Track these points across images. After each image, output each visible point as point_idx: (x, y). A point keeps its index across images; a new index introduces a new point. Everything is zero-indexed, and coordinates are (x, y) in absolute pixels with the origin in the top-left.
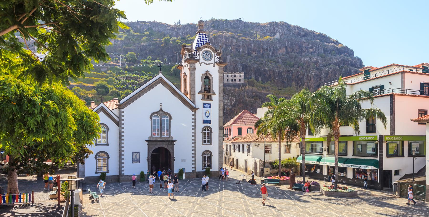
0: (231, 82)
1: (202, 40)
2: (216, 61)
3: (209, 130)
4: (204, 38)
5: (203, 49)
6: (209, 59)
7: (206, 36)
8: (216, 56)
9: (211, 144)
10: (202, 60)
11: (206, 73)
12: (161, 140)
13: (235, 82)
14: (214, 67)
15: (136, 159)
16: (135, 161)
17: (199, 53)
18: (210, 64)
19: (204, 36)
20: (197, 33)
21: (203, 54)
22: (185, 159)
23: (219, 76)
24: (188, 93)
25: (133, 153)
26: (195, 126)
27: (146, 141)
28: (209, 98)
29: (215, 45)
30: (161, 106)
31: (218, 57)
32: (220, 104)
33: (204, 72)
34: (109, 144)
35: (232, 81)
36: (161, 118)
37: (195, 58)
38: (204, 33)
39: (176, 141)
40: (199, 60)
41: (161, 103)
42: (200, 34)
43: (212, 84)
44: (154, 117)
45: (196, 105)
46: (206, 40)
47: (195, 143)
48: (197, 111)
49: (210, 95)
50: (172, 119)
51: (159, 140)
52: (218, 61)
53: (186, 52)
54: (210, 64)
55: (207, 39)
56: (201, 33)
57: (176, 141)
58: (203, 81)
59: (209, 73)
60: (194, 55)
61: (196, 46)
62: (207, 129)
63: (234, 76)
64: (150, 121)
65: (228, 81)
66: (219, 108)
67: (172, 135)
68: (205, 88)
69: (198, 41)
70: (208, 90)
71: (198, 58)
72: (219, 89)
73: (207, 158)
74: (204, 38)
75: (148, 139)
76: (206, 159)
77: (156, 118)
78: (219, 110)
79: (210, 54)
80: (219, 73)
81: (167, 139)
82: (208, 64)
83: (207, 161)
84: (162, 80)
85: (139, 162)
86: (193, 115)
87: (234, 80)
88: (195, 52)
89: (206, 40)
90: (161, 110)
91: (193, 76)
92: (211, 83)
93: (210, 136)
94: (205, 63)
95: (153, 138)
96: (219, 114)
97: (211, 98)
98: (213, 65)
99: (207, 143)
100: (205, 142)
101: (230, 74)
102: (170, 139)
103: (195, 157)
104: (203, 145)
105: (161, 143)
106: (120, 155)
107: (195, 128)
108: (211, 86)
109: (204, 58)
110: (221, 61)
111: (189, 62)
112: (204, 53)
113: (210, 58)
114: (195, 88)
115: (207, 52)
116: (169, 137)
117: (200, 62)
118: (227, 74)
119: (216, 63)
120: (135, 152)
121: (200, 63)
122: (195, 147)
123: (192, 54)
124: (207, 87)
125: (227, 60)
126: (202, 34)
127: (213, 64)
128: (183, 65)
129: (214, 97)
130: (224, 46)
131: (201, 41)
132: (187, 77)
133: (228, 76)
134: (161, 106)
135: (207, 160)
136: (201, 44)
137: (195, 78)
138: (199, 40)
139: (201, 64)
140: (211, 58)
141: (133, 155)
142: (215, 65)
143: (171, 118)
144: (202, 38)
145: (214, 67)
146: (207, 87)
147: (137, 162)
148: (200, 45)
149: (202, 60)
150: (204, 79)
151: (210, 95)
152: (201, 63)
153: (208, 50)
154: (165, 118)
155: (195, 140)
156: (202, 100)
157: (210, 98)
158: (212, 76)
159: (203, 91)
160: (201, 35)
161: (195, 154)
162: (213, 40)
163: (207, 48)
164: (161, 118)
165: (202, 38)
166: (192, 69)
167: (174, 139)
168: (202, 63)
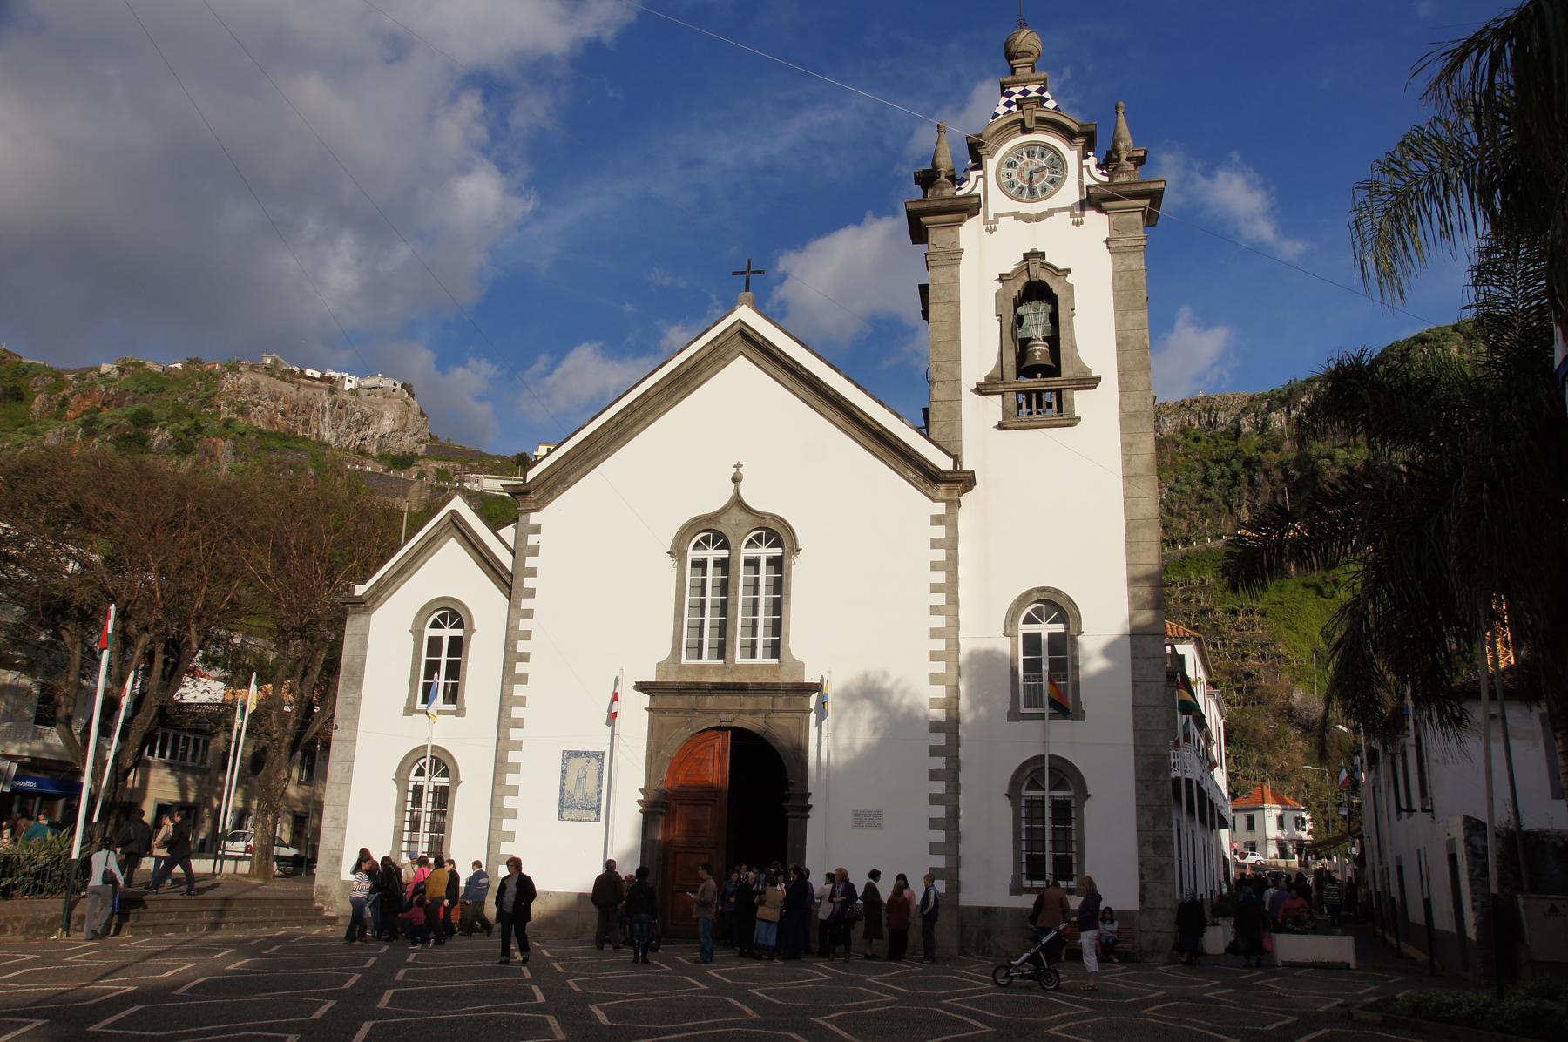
5: (1004, 141)
6: (1044, 189)
8: (1085, 162)
10: (998, 201)
12: (728, 680)
15: (578, 796)
16: (577, 807)
18: (1051, 212)
21: (1005, 170)
22: (879, 812)
23: (1115, 273)
25: (569, 755)
26: (951, 588)
30: (736, 479)
33: (1011, 263)
34: (465, 709)
41: (738, 466)
43: (1070, 323)
49: (1059, 393)
50: (799, 550)
51: (715, 679)
54: (1051, 212)
59: (1047, 260)
64: (669, 567)
66: (1127, 462)
70: (1049, 362)
72: (1118, 345)
73: (1048, 813)
75: (650, 677)
78: (1128, 478)
81: (762, 679)
82: (1039, 218)
85: (593, 814)
86: (937, 520)
90: (738, 502)
94: (1017, 215)
95: (684, 668)
96: (1129, 501)
98: (1072, 215)
99: (1047, 710)
102: (785, 678)
105: (727, 701)
107: (953, 600)
112: (1013, 165)
113: (1052, 182)
114: (957, 361)
117: (986, 215)
121: (986, 222)
124: (1040, 350)
129: (1081, 401)
134: (736, 479)
137: (957, 305)
139: (996, 221)
141: (564, 771)
146: (1040, 350)
147: (583, 813)
149: (998, 201)
152: (991, 217)
153: (1036, 144)
158: (1070, 279)
163: (1025, 131)
168: (997, 216)
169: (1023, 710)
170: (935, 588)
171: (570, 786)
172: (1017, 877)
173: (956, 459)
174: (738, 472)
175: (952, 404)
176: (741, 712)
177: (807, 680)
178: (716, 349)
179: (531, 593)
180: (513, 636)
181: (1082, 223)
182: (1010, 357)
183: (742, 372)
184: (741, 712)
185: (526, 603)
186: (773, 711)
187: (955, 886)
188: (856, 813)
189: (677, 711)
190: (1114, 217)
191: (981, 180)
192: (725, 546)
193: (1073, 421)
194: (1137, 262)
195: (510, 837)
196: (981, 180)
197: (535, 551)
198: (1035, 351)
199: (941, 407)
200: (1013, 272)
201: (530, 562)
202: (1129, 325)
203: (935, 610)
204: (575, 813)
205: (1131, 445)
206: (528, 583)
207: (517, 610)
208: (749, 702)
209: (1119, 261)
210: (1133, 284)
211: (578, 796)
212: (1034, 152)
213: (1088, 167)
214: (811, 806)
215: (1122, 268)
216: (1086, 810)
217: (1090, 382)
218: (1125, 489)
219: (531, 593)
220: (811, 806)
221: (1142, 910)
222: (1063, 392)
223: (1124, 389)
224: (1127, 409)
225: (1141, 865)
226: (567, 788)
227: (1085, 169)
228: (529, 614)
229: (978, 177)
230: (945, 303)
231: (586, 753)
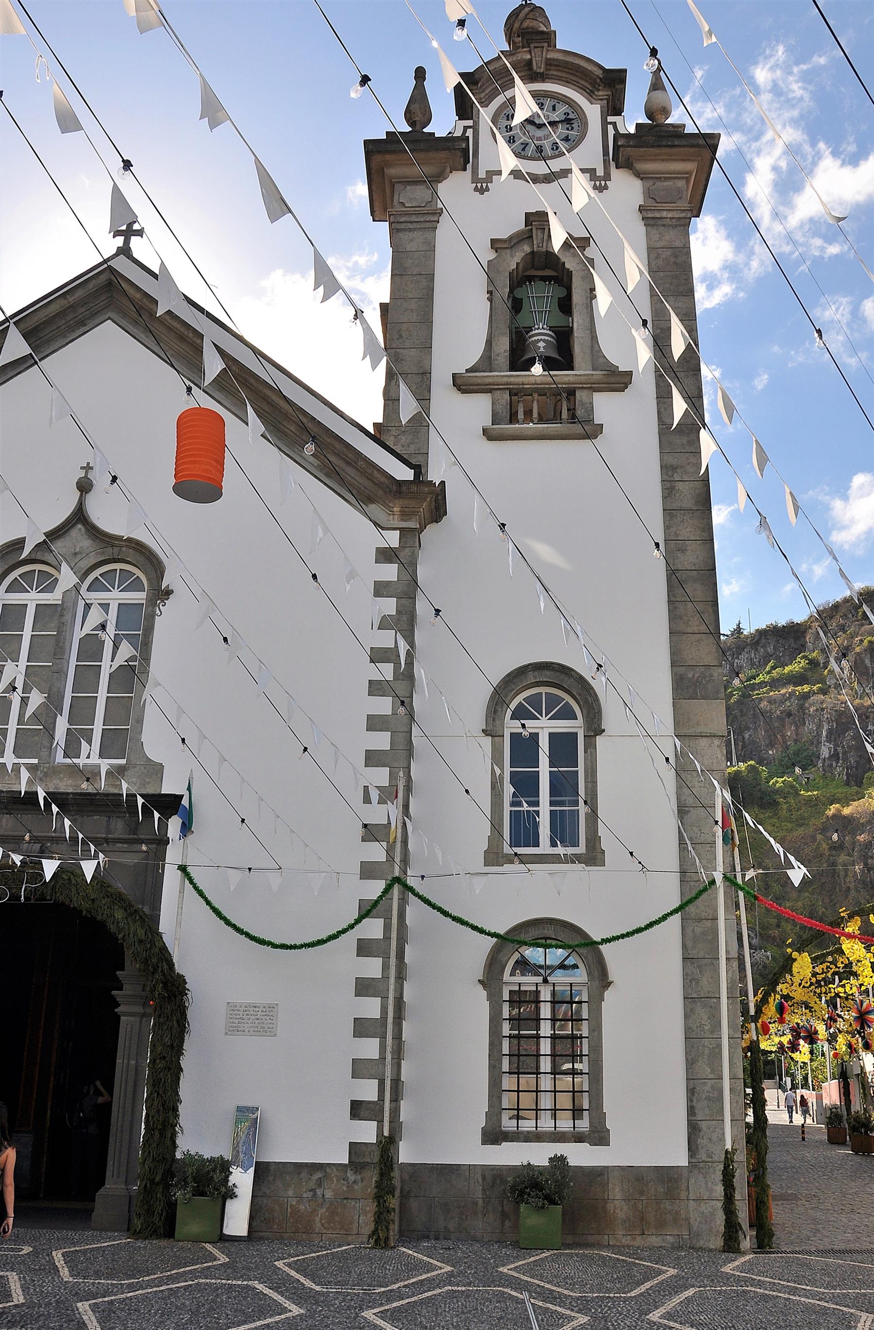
3: (567, 714)
11: (531, 237)
22: (272, 1007)
30: (84, 487)
32: (671, 460)
41: (88, 468)
49: (571, 393)
58: (496, 295)
62: (552, 701)
76: (537, 1020)
78: (669, 513)
83: (545, 1047)
86: (385, 555)
93: (581, 769)
97: (579, 412)
113: (566, 139)
114: (427, 347)
121: (475, 179)
134: (84, 487)
135: (546, 1029)
137: (431, 277)
142: (607, 177)
151: (571, 393)
152: (482, 175)
169: (507, 850)
173: (419, 470)
174: (86, 477)
178: (72, 307)
182: (503, 345)
190: (650, 183)
198: (539, 341)
200: (511, 238)
205: (674, 468)
209: (656, 237)
216: (606, 1006)
221: (692, 1165)
227: (610, 127)
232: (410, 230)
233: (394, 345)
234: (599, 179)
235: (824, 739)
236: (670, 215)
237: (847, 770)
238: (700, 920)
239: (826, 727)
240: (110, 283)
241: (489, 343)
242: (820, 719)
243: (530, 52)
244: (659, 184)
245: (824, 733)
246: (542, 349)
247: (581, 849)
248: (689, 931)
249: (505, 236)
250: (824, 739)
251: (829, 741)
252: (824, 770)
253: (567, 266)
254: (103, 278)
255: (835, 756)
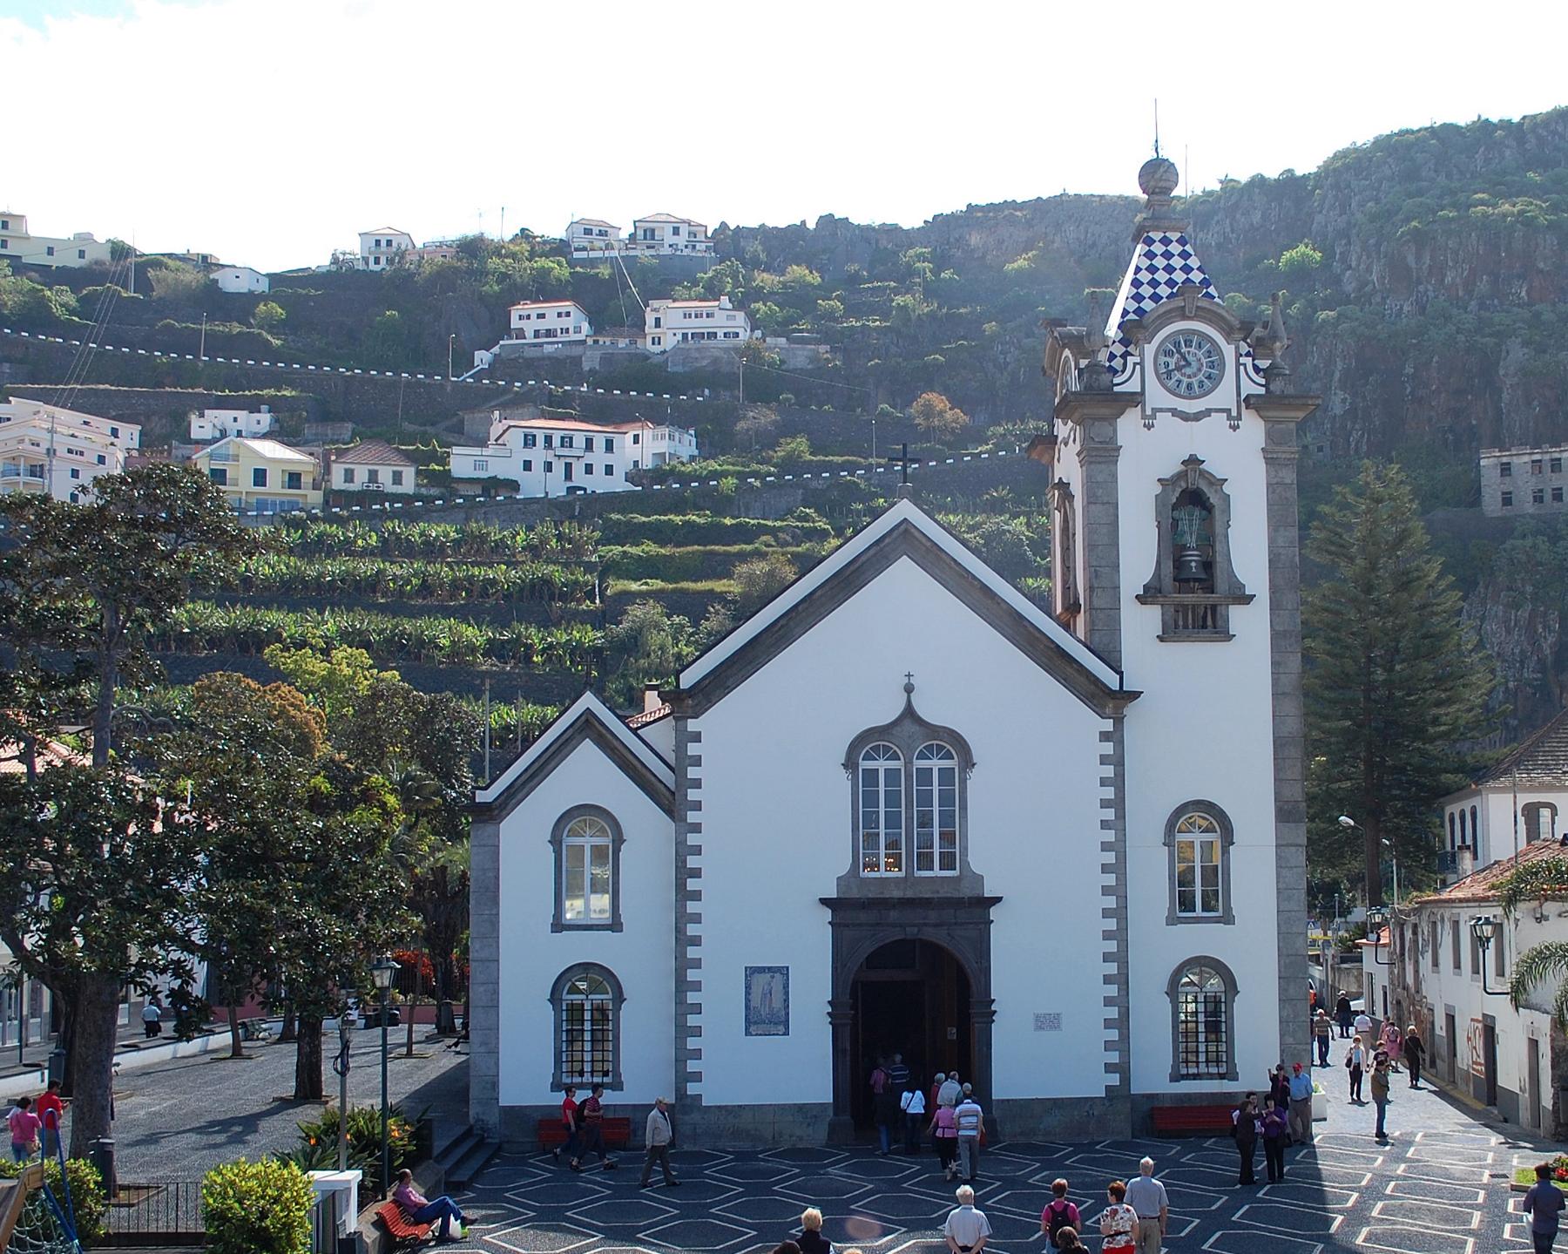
0: (1530, 508)
1: (1162, 276)
2: (1249, 388)
4: (1177, 262)
6: (1201, 383)
7: (1188, 248)
8: (1242, 360)
9: (1228, 919)
10: (1157, 395)
12: (909, 894)
13: (1556, 504)
14: (1235, 428)
15: (764, 1012)
17: (1142, 355)
18: (1208, 412)
19: (1175, 248)
20: (1136, 240)
21: (1162, 359)
23: (1269, 485)
24: (1082, 602)
25: (751, 972)
26: (1118, 803)
27: (825, 902)
28: (1204, 626)
29: (1421, 288)
30: (909, 689)
31: (1264, 364)
33: (1171, 468)
35: (1538, 498)
36: (909, 763)
37: (1116, 389)
38: (1174, 230)
39: (999, 899)
40: (1136, 399)
41: (909, 675)
42: (1150, 242)
44: (867, 757)
45: (1121, 674)
46: (1187, 269)
47: (1120, 913)
48: (1132, 711)
49: (1214, 608)
51: (897, 894)
52: (1262, 391)
53: (1067, 359)
54: (1208, 412)
55: (1194, 262)
56: (1156, 236)
57: (999, 899)
60: (1114, 372)
61: (1125, 313)
63: (1547, 468)
65: (1507, 500)
67: (977, 863)
68: (1179, 564)
69: (1136, 283)
70: (1203, 576)
71: (1133, 386)
74: (1177, 262)
77: (882, 765)
78: (1276, 695)
79: (1215, 349)
80: (1269, 461)
81: (945, 892)
82: (1197, 417)
84: (911, 534)
85: (781, 1029)
86: (1105, 737)
87: (1548, 497)
88: (1118, 350)
89: (1187, 269)
90: (909, 712)
91: (1103, 496)
92: (1218, 529)
94: (1175, 412)
97: (1219, 623)
98: (1229, 418)
99: (1199, 912)
100: (1186, 902)
101: (1522, 460)
102: (966, 892)
103: (1121, 1002)
104: (1172, 920)
106: (683, 986)
107: (1121, 815)
108: (1218, 547)
109: (1171, 383)
110: (1277, 386)
111: (1076, 415)
112: (1168, 353)
113: (1209, 377)
114: (1116, 567)
115: (1188, 343)
116: (957, 879)
117: (1143, 410)
118: (1505, 460)
119: (1249, 402)
120: (761, 970)
121: (1144, 417)
122: (1120, 935)
123: (1094, 368)
124: (1193, 559)
125: (1502, 372)
126: (1166, 241)
127: (1228, 411)
128: (1057, 436)
129: (1238, 616)
130: (1483, 285)
131: (1154, 283)
132: (1072, 506)
133: (1506, 469)
134: (909, 689)
136: (1155, 298)
138: (1145, 276)
140: (1215, 380)
141: (748, 987)
142: (1239, 417)
143: (968, 763)
144: (1160, 262)
145: (1235, 428)
146: (1193, 559)
148: (1148, 305)
149: (1157, 395)
150: (1174, 507)
152: (1149, 412)
153: (1194, 332)
154: (936, 764)
155: (1118, 891)
156: (1161, 639)
157: (1215, 628)
158: (1226, 488)
159: (1168, 582)
160: (1158, 248)
161: (1122, 980)
162: (1411, 260)
163: (1185, 317)
164: (909, 763)
165: (1160, 262)
166: (1101, 455)
167: (988, 893)
170: (1105, 804)
171: (756, 1000)
172: (1175, 1067)
175: (1112, 612)
176: (925, 924)
177: (986, 895)
179: (697, 806)
180: (683, 851)
181: (1238, 427)
182: (1169, 567)
183: (904, 570)
184: (925, 924)
185: (692, 817)
186: (955, 924)
187: (1126, 1080)
188: (1037, 1017)
189: (860, 925)
191: (1138, 367)
192: (895, 757)
193: (1229, 637)
194: (1289, 476)
195: (697, 1055)
196: (1138, 367)
197: (697, 761)
198: (1191, 561)
199: (1101, 616)
201: (692, 773)
202: (1280, 542)
203: (1105, 825)
204: (762, 1028)
206: (693, 794)
207: (683, 824)
208: (933, 916)
210: (1286, 498)
211: (764, 1012)
212: (1191, 342)
213: (1245, 365)
214: (995, 1012)
215: (1275, 481)
217: (1247, 599)
218: (1274, 707)
219: (697, 806)
220: (995, 1012)
222: (1219, 608)
223: (1275, 606)
224: (1277, 628)
225: (1282, 1051)
226: (752, 1004)
227: (1242, 368)
228: (697, 828)
229: (1135, 364)
230: (1103, 504)
231: (770, 969)
232: (1099, 463)
233: (1095, 564)
234: (1234, 419)
235: (1335, 383)
236: (1284, 456)
237: (1369, 435)
238: (1288, 956)
239: (1340, 365)
240: (906, 530)
241: (1158, 563)
242: (1330, 351)
243: (1184, 300)
244: (1277, 426)
245: (1337, 375)
246: (1194, 570)
247: (1220, 913)
248: (1282, 962)
249: (1167, 476)
250: (1335, 383)
251: (1343, 388)
252: (1333, 434)
253: (1212, 501)
254: (903, 527)
255: (1352, 413)
